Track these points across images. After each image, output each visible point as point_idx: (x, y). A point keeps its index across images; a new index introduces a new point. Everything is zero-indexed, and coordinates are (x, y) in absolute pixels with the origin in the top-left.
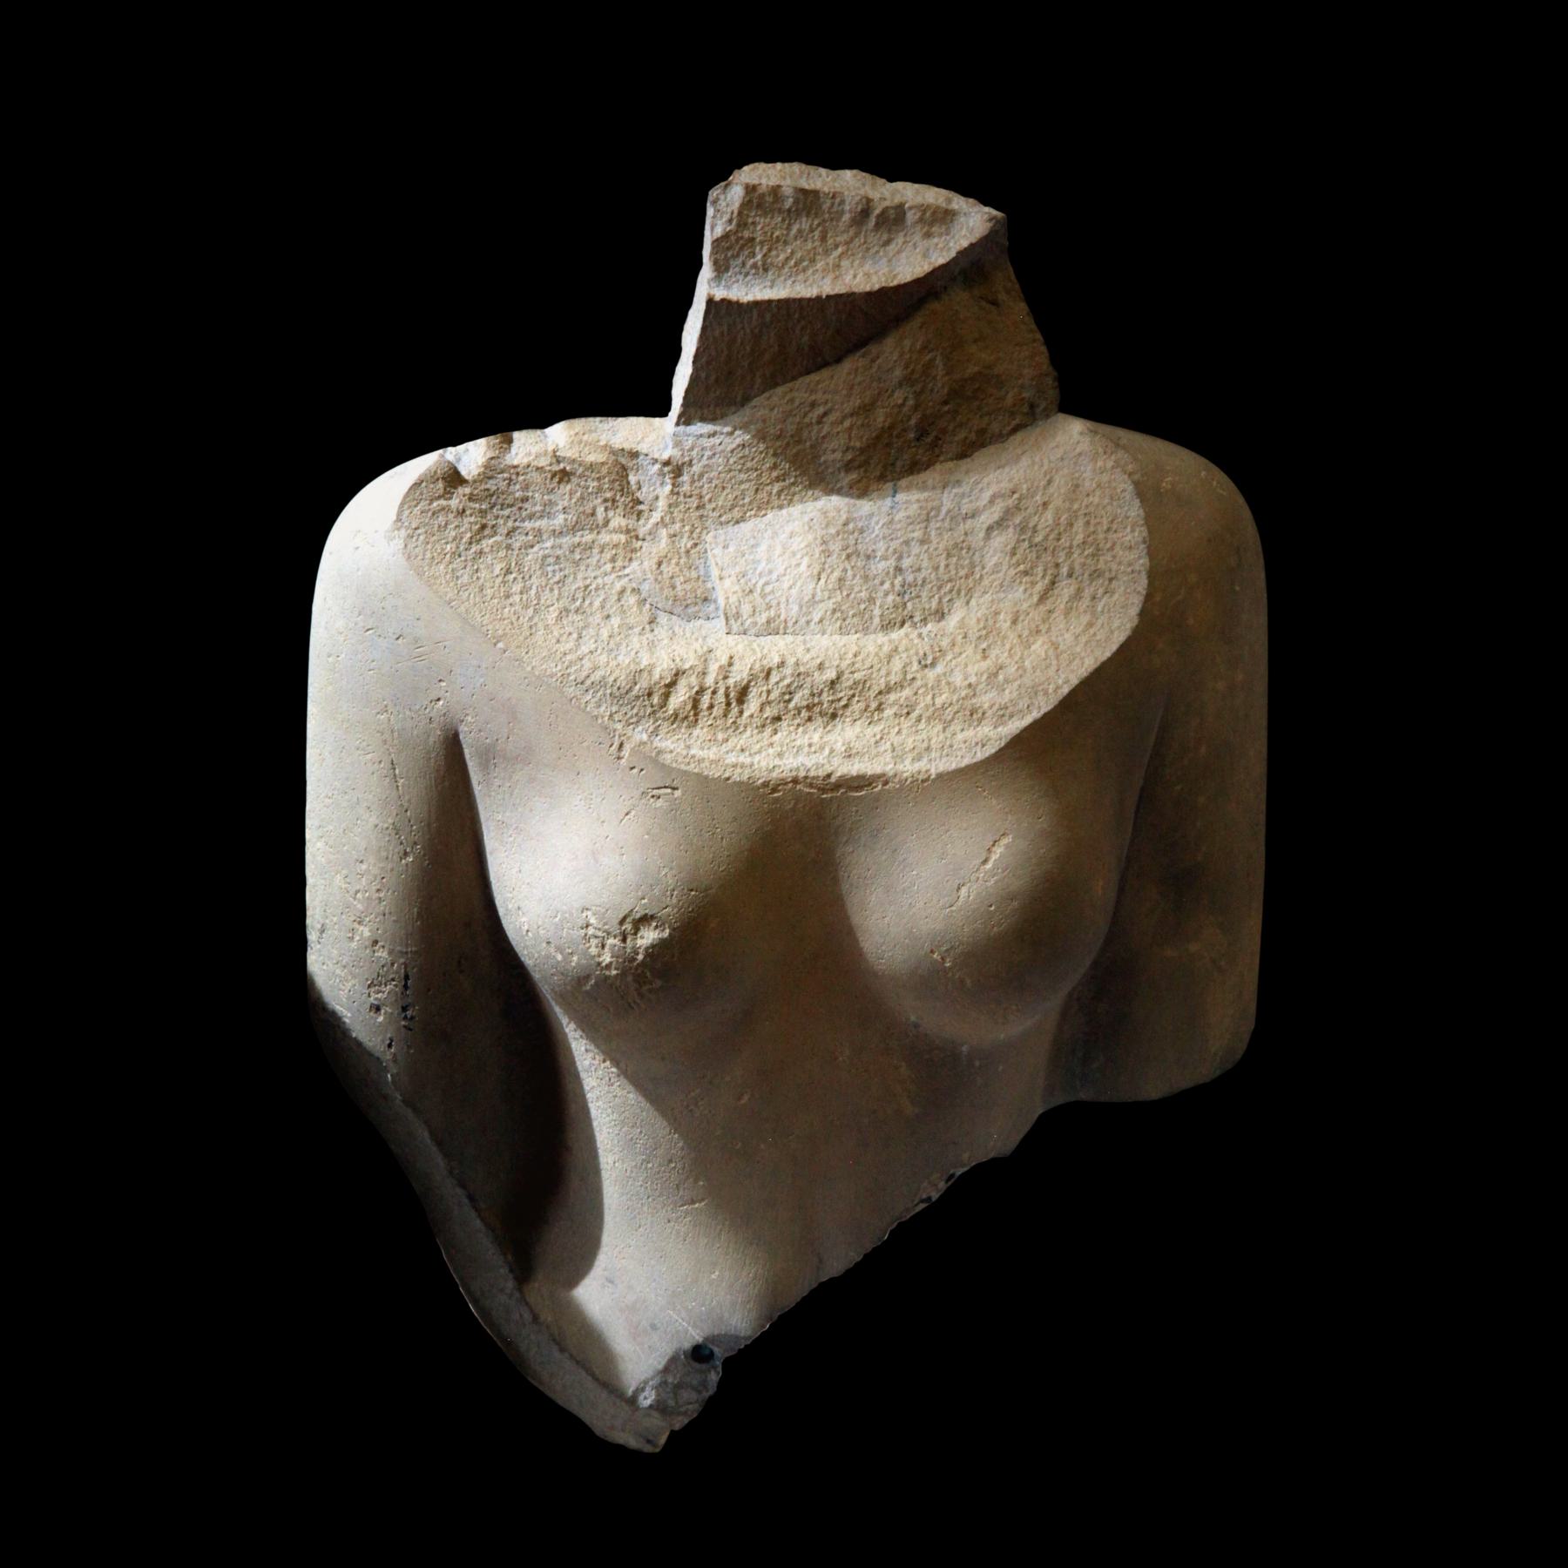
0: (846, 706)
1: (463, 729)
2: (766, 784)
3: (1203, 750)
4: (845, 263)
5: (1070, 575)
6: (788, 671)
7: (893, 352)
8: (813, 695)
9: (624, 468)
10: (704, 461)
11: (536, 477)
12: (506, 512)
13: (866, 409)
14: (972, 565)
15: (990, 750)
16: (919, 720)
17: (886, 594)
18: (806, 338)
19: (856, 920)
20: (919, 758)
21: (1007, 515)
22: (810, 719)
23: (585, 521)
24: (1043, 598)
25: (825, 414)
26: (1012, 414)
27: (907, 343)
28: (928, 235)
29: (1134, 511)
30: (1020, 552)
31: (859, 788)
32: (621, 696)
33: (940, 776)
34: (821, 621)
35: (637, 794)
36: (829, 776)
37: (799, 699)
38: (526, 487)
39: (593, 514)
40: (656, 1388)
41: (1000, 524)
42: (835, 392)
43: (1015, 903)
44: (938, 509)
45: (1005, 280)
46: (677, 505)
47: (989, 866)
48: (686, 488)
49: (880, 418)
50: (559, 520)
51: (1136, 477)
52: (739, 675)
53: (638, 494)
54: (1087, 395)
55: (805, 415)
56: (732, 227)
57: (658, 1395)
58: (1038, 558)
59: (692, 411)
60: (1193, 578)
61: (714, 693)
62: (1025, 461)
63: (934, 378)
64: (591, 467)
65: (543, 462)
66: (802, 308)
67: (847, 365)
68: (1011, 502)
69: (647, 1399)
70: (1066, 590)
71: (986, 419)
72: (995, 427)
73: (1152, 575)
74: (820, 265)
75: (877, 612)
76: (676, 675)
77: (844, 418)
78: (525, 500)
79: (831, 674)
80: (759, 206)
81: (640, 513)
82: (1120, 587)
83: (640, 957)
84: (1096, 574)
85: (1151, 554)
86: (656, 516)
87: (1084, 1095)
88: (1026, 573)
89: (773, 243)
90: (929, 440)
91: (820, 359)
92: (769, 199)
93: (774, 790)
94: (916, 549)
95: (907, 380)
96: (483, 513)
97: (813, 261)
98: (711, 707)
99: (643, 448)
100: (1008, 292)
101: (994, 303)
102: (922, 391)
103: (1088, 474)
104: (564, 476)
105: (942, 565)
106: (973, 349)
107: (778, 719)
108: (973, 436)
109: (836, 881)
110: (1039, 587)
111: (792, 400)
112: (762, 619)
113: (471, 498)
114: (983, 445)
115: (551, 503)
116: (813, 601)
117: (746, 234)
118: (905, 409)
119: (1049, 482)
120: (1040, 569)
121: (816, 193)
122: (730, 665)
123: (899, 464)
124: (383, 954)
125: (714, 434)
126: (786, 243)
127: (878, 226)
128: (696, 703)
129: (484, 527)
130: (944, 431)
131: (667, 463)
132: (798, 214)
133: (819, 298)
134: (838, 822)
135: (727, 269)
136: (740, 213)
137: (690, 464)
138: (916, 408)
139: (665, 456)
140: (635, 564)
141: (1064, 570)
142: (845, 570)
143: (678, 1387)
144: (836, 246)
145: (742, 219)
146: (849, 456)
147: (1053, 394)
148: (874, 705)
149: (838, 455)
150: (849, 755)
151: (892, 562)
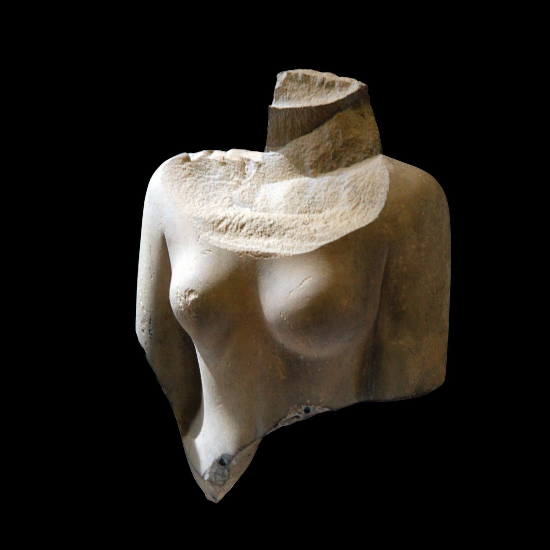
0: (273, 233)
1: (165, 233)
2: (238, 253)
3: (405, 269)
4: (313, 98)
5: (363, 202)
6: (258, 220)
7: (327, 128)
8: (264, 228)
9: (245, 164)
10: (269, 163)
11: (215, 163)
12: (201, 172)
13: (317, 147)
14: (337, 198)
15: (312, 249)
16: (294, 239)
17: (305, 204)
18: (299, 122)
19: (262, 303)
20: (289, 250)
21: (352, 182)
22: (261, 236)
23: (227, 177)
24: (354, 208)
25: (306, 149)
26: (365, 153)
27: (331, 126)
28: (341, 90)
29: (387, 182)
30: (351, 194)
31: (267, 257)
32: (205, 222)
33: (293, 256)
34: (280, 210)
35: (200, 252)
36: (258, 252)
37: (259, 229)
38: (211, 166)
39: (229, 175)
40: (209, 473)
41: (348, 186)
42: (309, 141)
43: (308, 300)
44: (333, 182)
45: (368, 109)
46: (256, 176)
47: (302, 286)
48: (261, 171)
49: (321, 151)
50: (217, 177)
51: (392, 172)
52: (244, 220)
53: (246, 172)
54: (390, 149)
55: (300, 149)
56: (281, 85)
57: (210, 476)
58: (356, 196)
59: (269, 147)
60: (403, 206)
61: (234, 224)
62: (363, 167)
63: (339, 138)
64: (233, 162)
65: (218, 159)
66: (297, 112)
67: (314, 133)
68: (353, 179)
69: (207, 477)
70: (361, 206)
71: (356, 154)
72: (359, 157)
73: (386, 203)
74: (306, 98)
75: (299, 208)
76: (224, 218)
77: (311, 150)
78: (209, 169)
79: (271, 222)
80: (291, 79)
81: (244, 178)
82: (376, 206)
83: (189, 304)
84: (371, 202)
85: (388, 196)
86: (249, 179)
87: (371, 398)
88: (351, 201)
89: (293, 90)
90: (337, 160)
91: (305, 131)
92: (294, 77)
93: (240, 255)
94: (322, 193)
95: (330, 138)
96: (192, 170)
97: (303, 97)
98: (232, 228)
99: (251, 159)
100: (368, 112)
101: (363, 116)
102: (335, 142)
103: (378, 171)
104: (224, 164)
105: (328, 196)
106: (353, 130)
107: (252, 235)
108: (351, 160)
109: (257, 289)
110: (353, 205)
111: (297, 145)
112: (262, 208)
113: (190, 166)
114: (354, 163)
115: (217, 171)
116: (281, 203)
117: (285, 88)
118: (329, 148)
119: (366, 173)
120: (355, 200)
121: (309, 76)
122: (243, 217)
123: (327, 168)
124: (145, 311)
125: (273, 155)
126: (296, 91)
127: (326, 87)
128: (227, 227)
129: (190, 174)
130: (342, 157)
131: (257, 163)
132: (303, 82)
133: (301, 108)
134: (259, 268)
135: (278, 99)
136: (284, 81)
137: (265, 164)
138: (332, 148)
139: (257, 161)
140: (235, 192)
141: (362, 200)
142: (295, 196)
143: (215, 474)
144: (312, 93)
145: (284, 83)
146: (311, 164)
147: (379, 146)
148: (282, 233)
149: (309, 163)
150: (268, 247)
151: (313, 195)
